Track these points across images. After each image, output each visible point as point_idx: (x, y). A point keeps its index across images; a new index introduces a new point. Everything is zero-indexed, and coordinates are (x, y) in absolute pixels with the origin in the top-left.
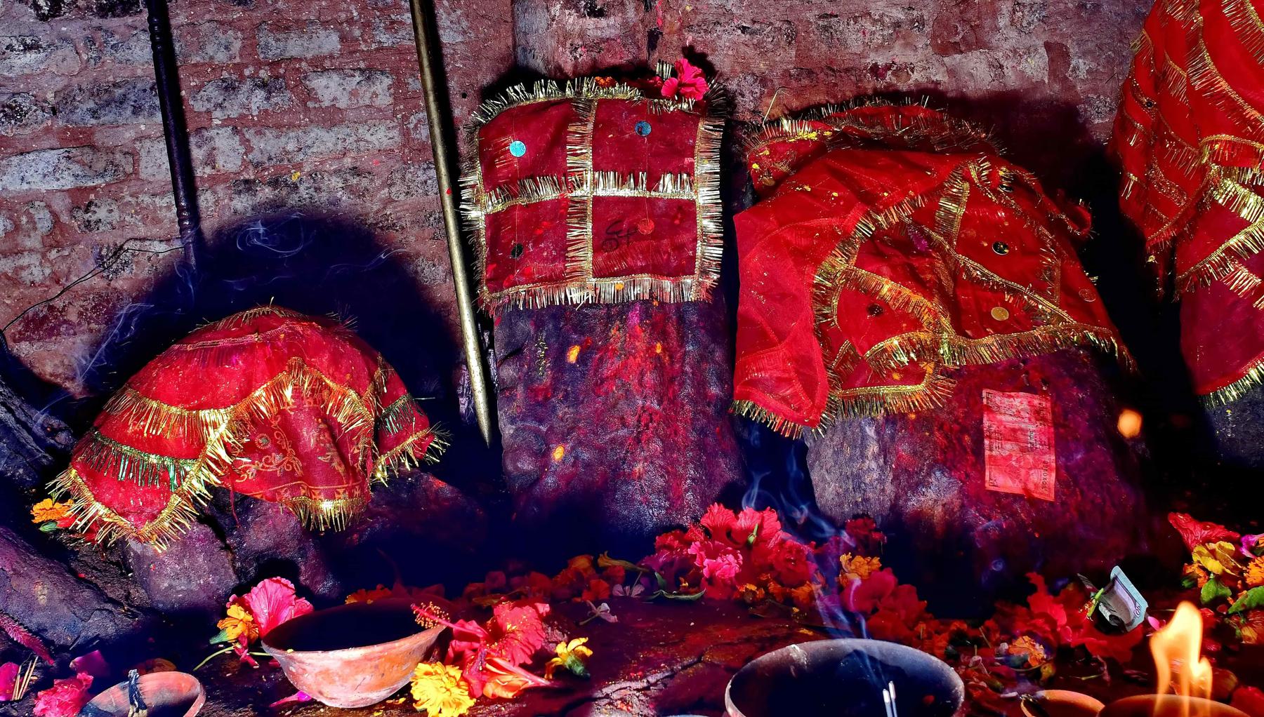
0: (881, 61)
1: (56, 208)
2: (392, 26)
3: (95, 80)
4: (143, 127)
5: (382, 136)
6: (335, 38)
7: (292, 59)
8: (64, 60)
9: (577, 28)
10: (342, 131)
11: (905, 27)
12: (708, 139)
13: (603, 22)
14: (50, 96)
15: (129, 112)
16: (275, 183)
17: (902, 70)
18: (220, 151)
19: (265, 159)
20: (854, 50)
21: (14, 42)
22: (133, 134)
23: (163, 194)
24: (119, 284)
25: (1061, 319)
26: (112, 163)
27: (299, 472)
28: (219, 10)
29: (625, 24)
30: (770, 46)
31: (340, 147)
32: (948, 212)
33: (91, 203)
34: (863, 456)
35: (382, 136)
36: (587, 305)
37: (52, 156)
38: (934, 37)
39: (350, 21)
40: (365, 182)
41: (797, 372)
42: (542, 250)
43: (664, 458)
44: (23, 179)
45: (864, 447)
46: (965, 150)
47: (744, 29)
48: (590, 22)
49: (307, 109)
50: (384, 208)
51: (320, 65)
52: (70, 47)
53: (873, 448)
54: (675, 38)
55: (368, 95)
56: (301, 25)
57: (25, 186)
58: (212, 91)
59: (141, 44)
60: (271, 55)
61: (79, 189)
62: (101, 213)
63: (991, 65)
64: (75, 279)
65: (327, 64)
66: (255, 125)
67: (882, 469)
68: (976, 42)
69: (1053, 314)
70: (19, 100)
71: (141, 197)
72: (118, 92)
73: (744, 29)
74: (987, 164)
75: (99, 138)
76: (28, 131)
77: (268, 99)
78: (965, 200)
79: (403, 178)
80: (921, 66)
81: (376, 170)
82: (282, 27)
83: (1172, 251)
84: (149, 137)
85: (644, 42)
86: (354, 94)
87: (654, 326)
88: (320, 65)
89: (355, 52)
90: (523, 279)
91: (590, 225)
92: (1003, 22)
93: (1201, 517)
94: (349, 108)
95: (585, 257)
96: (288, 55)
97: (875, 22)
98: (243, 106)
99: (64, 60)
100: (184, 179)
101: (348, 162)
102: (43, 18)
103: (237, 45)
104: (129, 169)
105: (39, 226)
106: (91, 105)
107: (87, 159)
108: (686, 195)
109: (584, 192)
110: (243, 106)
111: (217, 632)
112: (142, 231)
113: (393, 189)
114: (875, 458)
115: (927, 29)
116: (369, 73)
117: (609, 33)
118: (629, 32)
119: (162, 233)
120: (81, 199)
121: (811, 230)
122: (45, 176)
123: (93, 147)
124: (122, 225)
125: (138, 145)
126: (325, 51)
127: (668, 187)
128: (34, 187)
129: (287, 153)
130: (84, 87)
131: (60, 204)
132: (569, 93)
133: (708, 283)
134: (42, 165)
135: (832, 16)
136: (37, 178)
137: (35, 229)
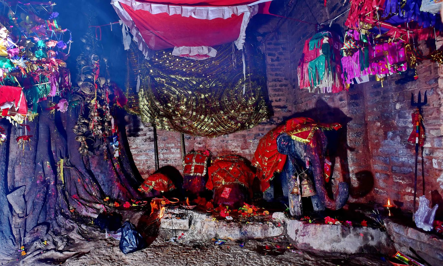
18: (161, 156)
51: (172, 148)
58: (160, 150)
82: (168, 143)
88: (172, 148)
100: (157, 159)
116: (177, 149)
118: (203, 146)
120: (147, 161)
131: (144, 161)
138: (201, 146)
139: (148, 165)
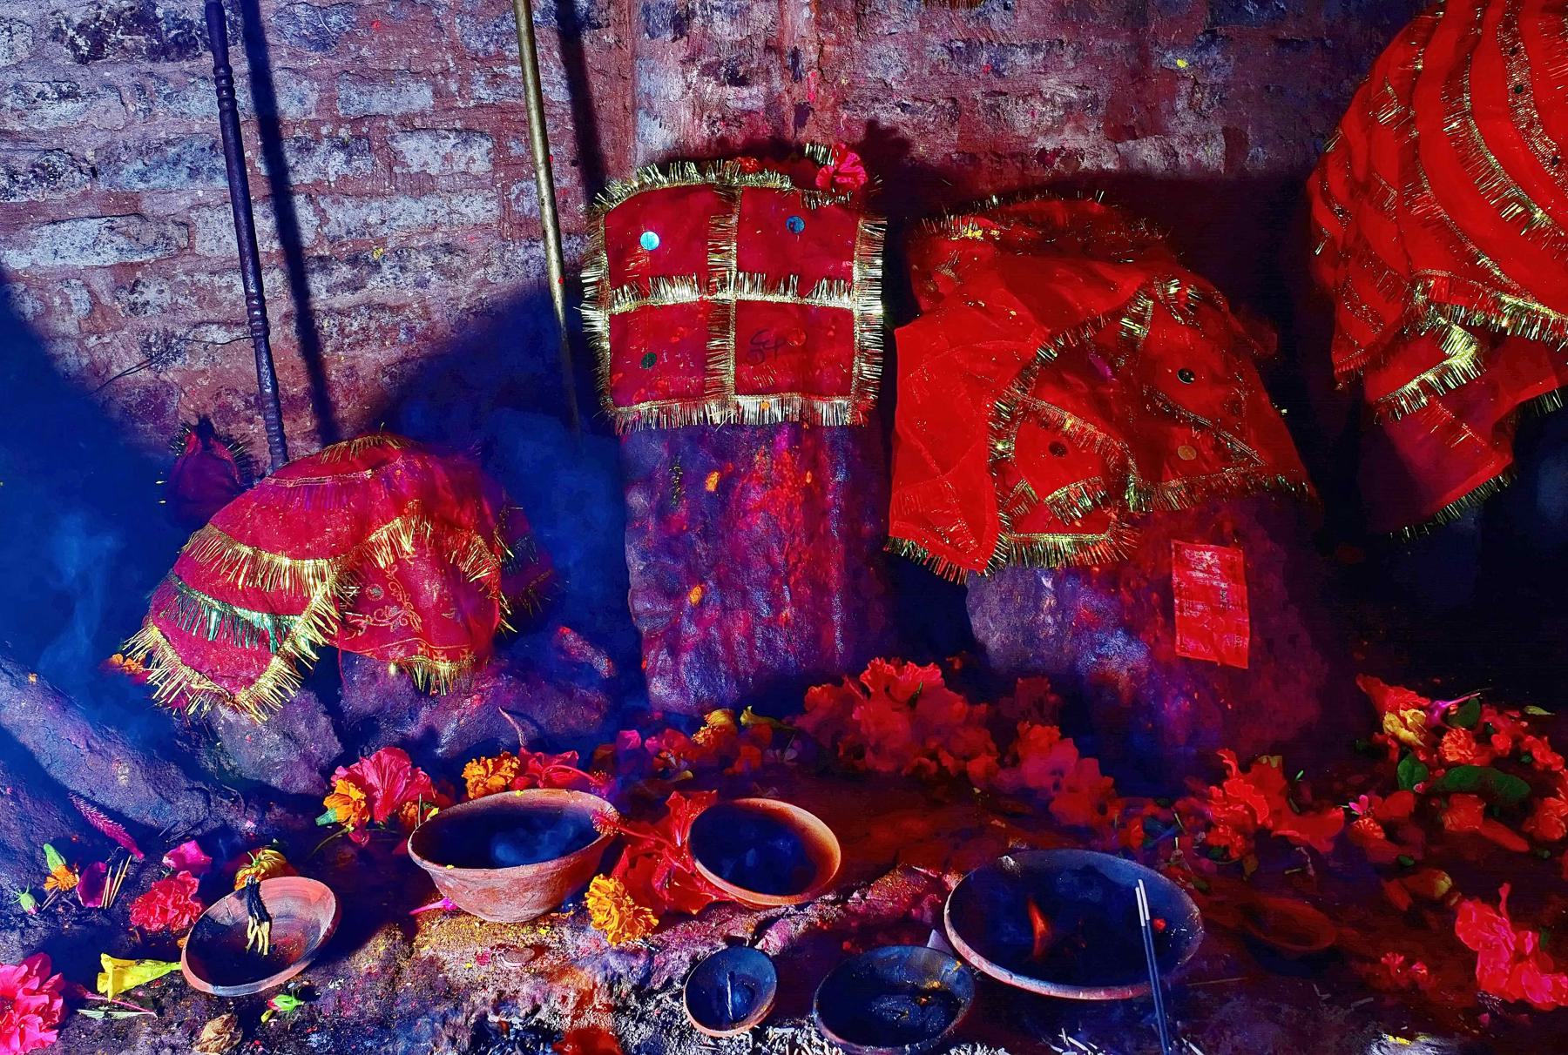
1: (95, 287)
2: (495, 80)
3: (144, 136)
4: (200, 193)
6: (427, 92)
7: (377, 116)
8: (107, 111)
9: (716, 97)
10: (433, 202)
13: (745, 92)
15: (184, 176)
16: (354, 261)
19: (343, 233)
20: (1022, 132)
21: (47, 88)
22: (189, 202)
25: (1251, 460)
26: (163, 235)
27: (417, 628)
28: (293, 55)
29: (770, 93)
30: (931, 127)
31: (429, 220)
32: (1130, 331)
33: (137, 282)
34: (1038, 609)
36: (728, 426)
39: (445, 73)
40: (457, 261)
44: (56, 253)
45: (1038, 598)
47: (904, 107)
48: (730, 91)
49: (392, 176)
50: (479, 291)
51: (408, 124)
52: (115, 96)
53: (1049, 601)
54: (828, 115)
55: (464, 160)
56: (387, 76)
57: (59, 262)
59: (200, 94)
60: (353, 112)
61: (124, 265)
62: (150, 294)
65: (418, 123)
66: (331, 193)
69: (1242, 454)
70: (54, 158)
71: (197, 276)
72: (172, 151)
73: (904, 107)
75: (146, 206)
76: (62, 196)
77: (348, 162)
82: (365, 77)
84: (207, 205)
86: (447, 158)
88: (408, 124)
89: (451, 109)
93: (1392, 681)
94: (441, 174)
95: (728, 370)
96: (372, 111)
97: (1045, 102)
98: (318, 170)
99: (107, 111)
101: (438, 237)
102: (83, 60)
103: (313, 98)
104: (184, 242)
105: (75, 308)
106: (139, 166)
107: (133, 230)
109: (729, 295)
110: (318, 170)
112: (198, 315)
113: (490, 270)
114: (1052, 612)
116: (467, 134)
117: (748, 105)
118: (773, 103)
119: (221, 317)
120: (126, 277)
122: (83, 249)
123: (139, 215)
124: (174, 308)
125: (194, 214)
128: (69, 262)
130: (130, 144)
131: (100, 283)
134: (80, 236)
136: (74, 252)
137: (71, 312)
138: (751, 97)
139: (154, 322)
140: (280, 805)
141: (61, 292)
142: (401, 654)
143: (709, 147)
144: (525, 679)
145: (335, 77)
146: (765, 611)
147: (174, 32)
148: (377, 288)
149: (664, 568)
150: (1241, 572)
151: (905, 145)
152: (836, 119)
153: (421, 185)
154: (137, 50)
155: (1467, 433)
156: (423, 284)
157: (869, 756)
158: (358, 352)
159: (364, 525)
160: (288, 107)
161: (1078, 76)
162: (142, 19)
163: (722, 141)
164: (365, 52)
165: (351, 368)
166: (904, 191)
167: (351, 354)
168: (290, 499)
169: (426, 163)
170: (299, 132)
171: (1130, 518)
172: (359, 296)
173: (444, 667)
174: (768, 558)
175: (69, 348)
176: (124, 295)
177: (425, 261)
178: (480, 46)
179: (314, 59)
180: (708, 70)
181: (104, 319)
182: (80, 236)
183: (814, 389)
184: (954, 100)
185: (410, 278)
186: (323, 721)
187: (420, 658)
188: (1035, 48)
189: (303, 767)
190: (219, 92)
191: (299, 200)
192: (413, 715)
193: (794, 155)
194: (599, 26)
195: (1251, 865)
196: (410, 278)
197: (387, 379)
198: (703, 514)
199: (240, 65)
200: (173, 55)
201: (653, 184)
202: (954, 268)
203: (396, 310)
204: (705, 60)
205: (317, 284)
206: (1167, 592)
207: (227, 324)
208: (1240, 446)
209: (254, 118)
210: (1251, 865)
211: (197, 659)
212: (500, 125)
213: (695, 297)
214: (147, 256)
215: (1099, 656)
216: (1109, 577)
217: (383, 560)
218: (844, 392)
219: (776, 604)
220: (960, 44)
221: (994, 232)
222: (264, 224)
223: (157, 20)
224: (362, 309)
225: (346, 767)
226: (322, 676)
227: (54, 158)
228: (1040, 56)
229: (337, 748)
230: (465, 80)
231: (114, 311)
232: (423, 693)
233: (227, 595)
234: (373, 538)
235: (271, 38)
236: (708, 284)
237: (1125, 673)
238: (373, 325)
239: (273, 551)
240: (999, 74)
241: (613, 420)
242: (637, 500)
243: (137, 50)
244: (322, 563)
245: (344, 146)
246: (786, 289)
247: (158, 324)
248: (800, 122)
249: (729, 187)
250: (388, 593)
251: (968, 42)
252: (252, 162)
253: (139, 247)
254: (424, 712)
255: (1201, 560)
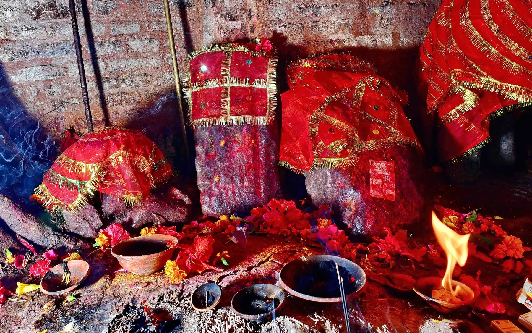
0: (334, 39)
1: (39, 87)
2: (159, 23)
4: (70, 58)
5: (155, 62)
6: (138, 27)
7: (123, 34)
9: (225, 25)
10: (141, 61)
11: (342, 26)
12: (272, 66)
13: (235, 23)
14: (37, 47)
16: (117, 79)
17: (341, 41)
20: (324, 34)
21: (24, 27)
23: (76, 83)
24: (61, 114)
25: (397, 134)
27: (125, 186)
28: (97, 16)
29: (243, 23)
30: (294, 33)
31: (140, 66)
34: (326, 182)
35: (155, 62)
36: (228, 126)
37: (37, 68)
38: (353, 30)
39: (144, 21)
40: (149, 79)
41: (302, 151)
42: (212, 106)
43: (255, 181)
45: (326, 179)
46: (363, 72)
47: (285, 26)
48: (230, 23)
51: (132, 37)
53: (329, 180)
54: (260, 29)
55: (150, 47)
57: (28, 79)
60: (116, 33)
62: (55, 89)
63: (373, 40)
64: (46, 113)
65: (136, 36)
67: (333, 187)
68: (368, 32)
70: (26, 48)
71: (69, 84)
72: (61, 46)
73: (285, 26)
74: (372, 77)
75: (53, 62)
76: (29, 59)
77: (114, 49)
78: (364, 90)
79: (162, 77)
80: (349, 40)
81: (153, 75)
82: (120, 23)
83: (437, 110)
85: (249, 31)
87: (252, 134)
89: (146, 32)
90: (205, 116)
91: (229, 97)
92: (377, 25)
94: (143, 52)
95: (227, 107)
96: (122, 33)
98: (105, 51)
101: (143, 71)
102: (34, 19)
103: (104, 29)
104: (65, 73)
106: (51, 50)
107: (50, 70)
108: (263, 86)
109: (228, 85)
110: (105, 51)
111: (95, 242)
112: (70, 96)
114: (330, 183)
115: (350, 27)
116: (151, 39)
117: (236, 27)
118: (243, 26)
119: (77, 96)
120: (48, 84)
121: (309, 100)
124: (62, 93)
125: (68, 65)
126: (135, 31)
127: (257, 85)
128: (31, 79)
129: (121, 68)
130: (48, 44)
131: (40, 86)
132: (223, 49)
133: (271, 118)
135: (317, 21)
136: (32, 76)
137: (31, 94)
138: (237, 25)
140: (82, 240)
141: (28, 89)
142: (120, 194)
143: (223, 41)
144: (160, 203)
145: (110, 23)
146: (239, 184)
147: (61, 10)
148: (124, 87)
149: (207, 170)
150: (393, 170)
151: (285, 38)
152: (263, 30)
153: (137, 56)
154: (50, 15)
155: (473, 126)
156: (138, 86)
157: (269, 229)
158: (118, 107)
159: (107, 153)
160: (96, 32)
161: (342, 16)
162: (52, 6)
163: (228, 38)
164: (119, 15)
165: (116, 112)
166: (284, 52)
167: (116, 107)
168: (85, 145)
169: (138, 49)
170: (99, 40)
171: (356, 153)
172: (119, 89)
173: (133, 198)
174: (240, 167)
175: (31, 105)
176: (47, 89)
177: (138, 79)
178: (154, 13)
179: (104, 17)
180: (223, 16)
181: (41, 96)
182: (34, 72)
183: (255, 113)
184: (302, 24)
185: (134, 84)
186: (96, 215)
187: (126, 195)
188: (328, 7)
189: (90, 229)
190: (73, 27)
191: (100, 61)
192: (125, 214)
193: (251, 42)
194: (191, 6)
195: (392, 263)
196: (134, 84)
197: (127, 115)
198: (219, 153)
199: (81, 19)
200: (61, 17)
201: (205, 51)
202: (301, 76)
203: (130, 94)
204: (222, 13)
205: (105, 85)
206: (368, 176)
207: (78, 98)
208: (394, 130)
209: (86, 35)
210: (392, 263)
211: (56, 194)
212: (160, 37)
213: (217, 86)
214: (54, 78)
215: (345, 197)
216: (348, 171)
217: (114, 164)
218: (264, 114)
219: (242, 181)
220: (303, 6)
221: (314, 65)
222: (88, 67)
223: (56, 6)
224: (119, 94)
225: (103, 229)
226: (96, 201)
227: (26, 48)
228: (329, 10)
229: (101, 224)
230: (150, 23)
231: (44, 94)
232: (128, 207)
233: (65, 174)
234: (110, 157)
235: (90, 11)
236: (221, 81)
237: (353, 202)
238: (123, 98)
239: (80, 161)
240: (316, 16)
241: (192, 125)
242: (199, 149)
243: (50, 15)
244: (94, 165)
245: (113, 43)
246: (246, 82)
247: (57, 98)
248: (252, 32)
249: (229, 51)
250: (116, 175)
251: (306, 6)
252: (84, 49)
253: (51, 75)
254: (129, 213)
255: (379, 166)
